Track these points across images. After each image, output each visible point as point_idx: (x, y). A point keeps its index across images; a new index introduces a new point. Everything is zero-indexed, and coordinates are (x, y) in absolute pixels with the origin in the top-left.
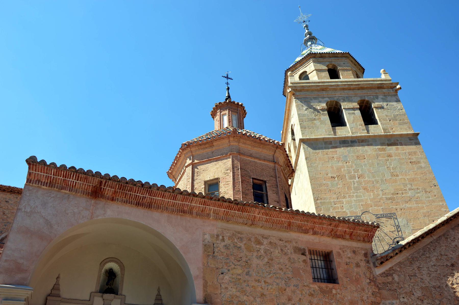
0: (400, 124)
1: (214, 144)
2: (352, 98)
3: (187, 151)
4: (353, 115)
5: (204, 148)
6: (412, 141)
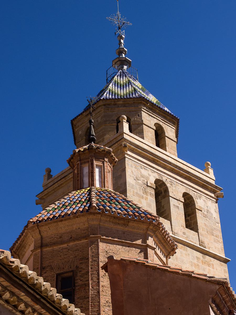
1: (130, 224)
3: (95, 217)
4: (177, 210)
5: (116, 223)
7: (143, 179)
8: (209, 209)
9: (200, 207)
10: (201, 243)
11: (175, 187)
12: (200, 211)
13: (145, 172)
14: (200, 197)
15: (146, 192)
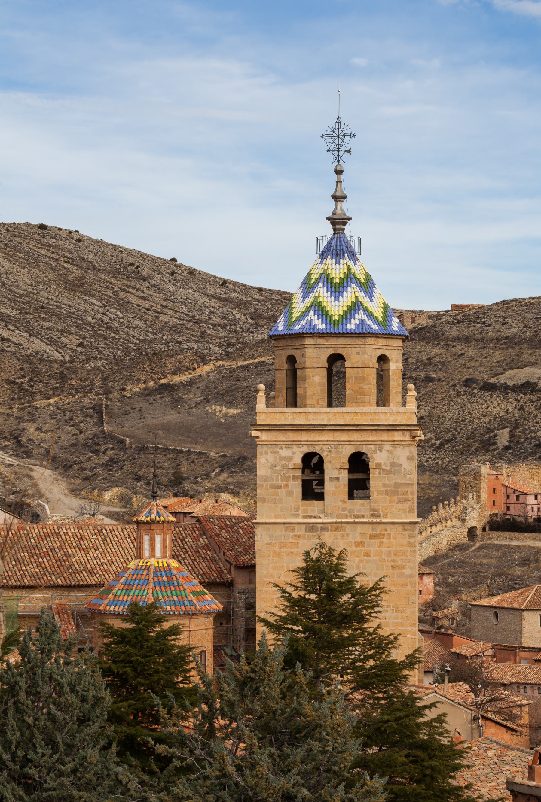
0: (399, 502)
2: (342, 448)
4: (335, 483)
6: (404, 533)
7: (283, 462)
8: (395, 460)
9: (376, 464)
10: (374, 513)
11: (336, 452)
12: (377, 470)
13: (285, 453)
14: (381, 451)
15: (287, 479)
